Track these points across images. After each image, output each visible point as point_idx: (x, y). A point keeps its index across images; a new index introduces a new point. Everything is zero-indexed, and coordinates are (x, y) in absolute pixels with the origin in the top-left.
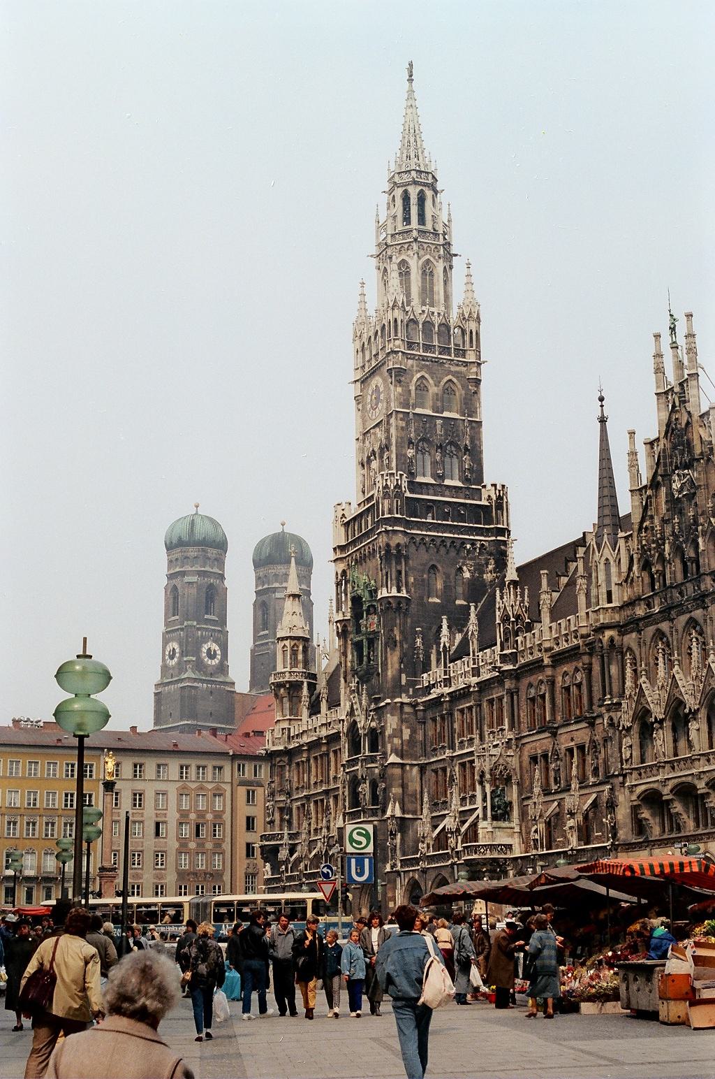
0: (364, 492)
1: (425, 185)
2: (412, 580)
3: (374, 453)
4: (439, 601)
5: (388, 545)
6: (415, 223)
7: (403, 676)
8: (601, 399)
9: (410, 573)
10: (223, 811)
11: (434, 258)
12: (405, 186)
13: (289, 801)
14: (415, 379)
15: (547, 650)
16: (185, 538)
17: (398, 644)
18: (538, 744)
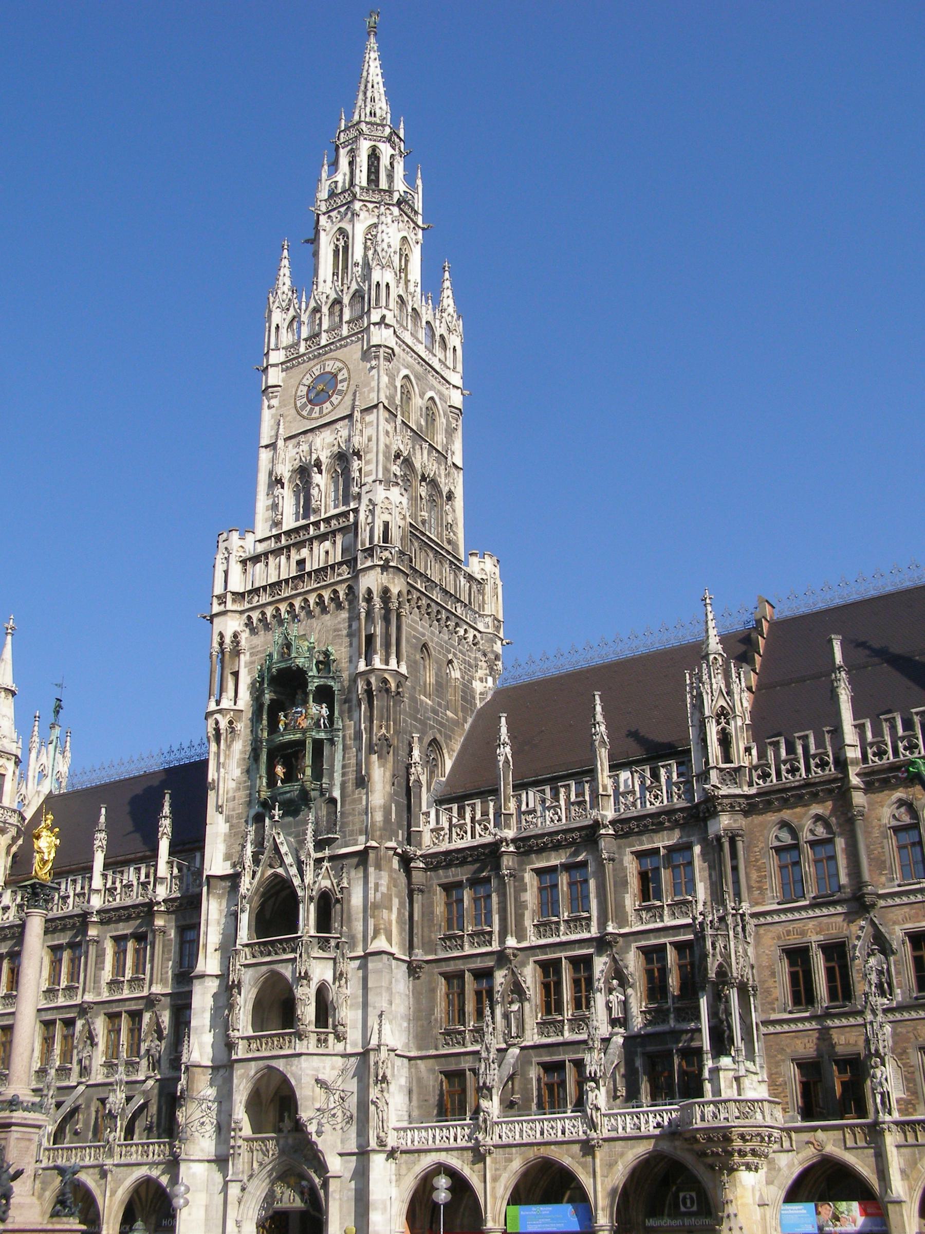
0: (277, 524)
3: (318, 464)
4: (430, 702)
5: (386, 591)
12: (375, 140)
18: (811, 924)
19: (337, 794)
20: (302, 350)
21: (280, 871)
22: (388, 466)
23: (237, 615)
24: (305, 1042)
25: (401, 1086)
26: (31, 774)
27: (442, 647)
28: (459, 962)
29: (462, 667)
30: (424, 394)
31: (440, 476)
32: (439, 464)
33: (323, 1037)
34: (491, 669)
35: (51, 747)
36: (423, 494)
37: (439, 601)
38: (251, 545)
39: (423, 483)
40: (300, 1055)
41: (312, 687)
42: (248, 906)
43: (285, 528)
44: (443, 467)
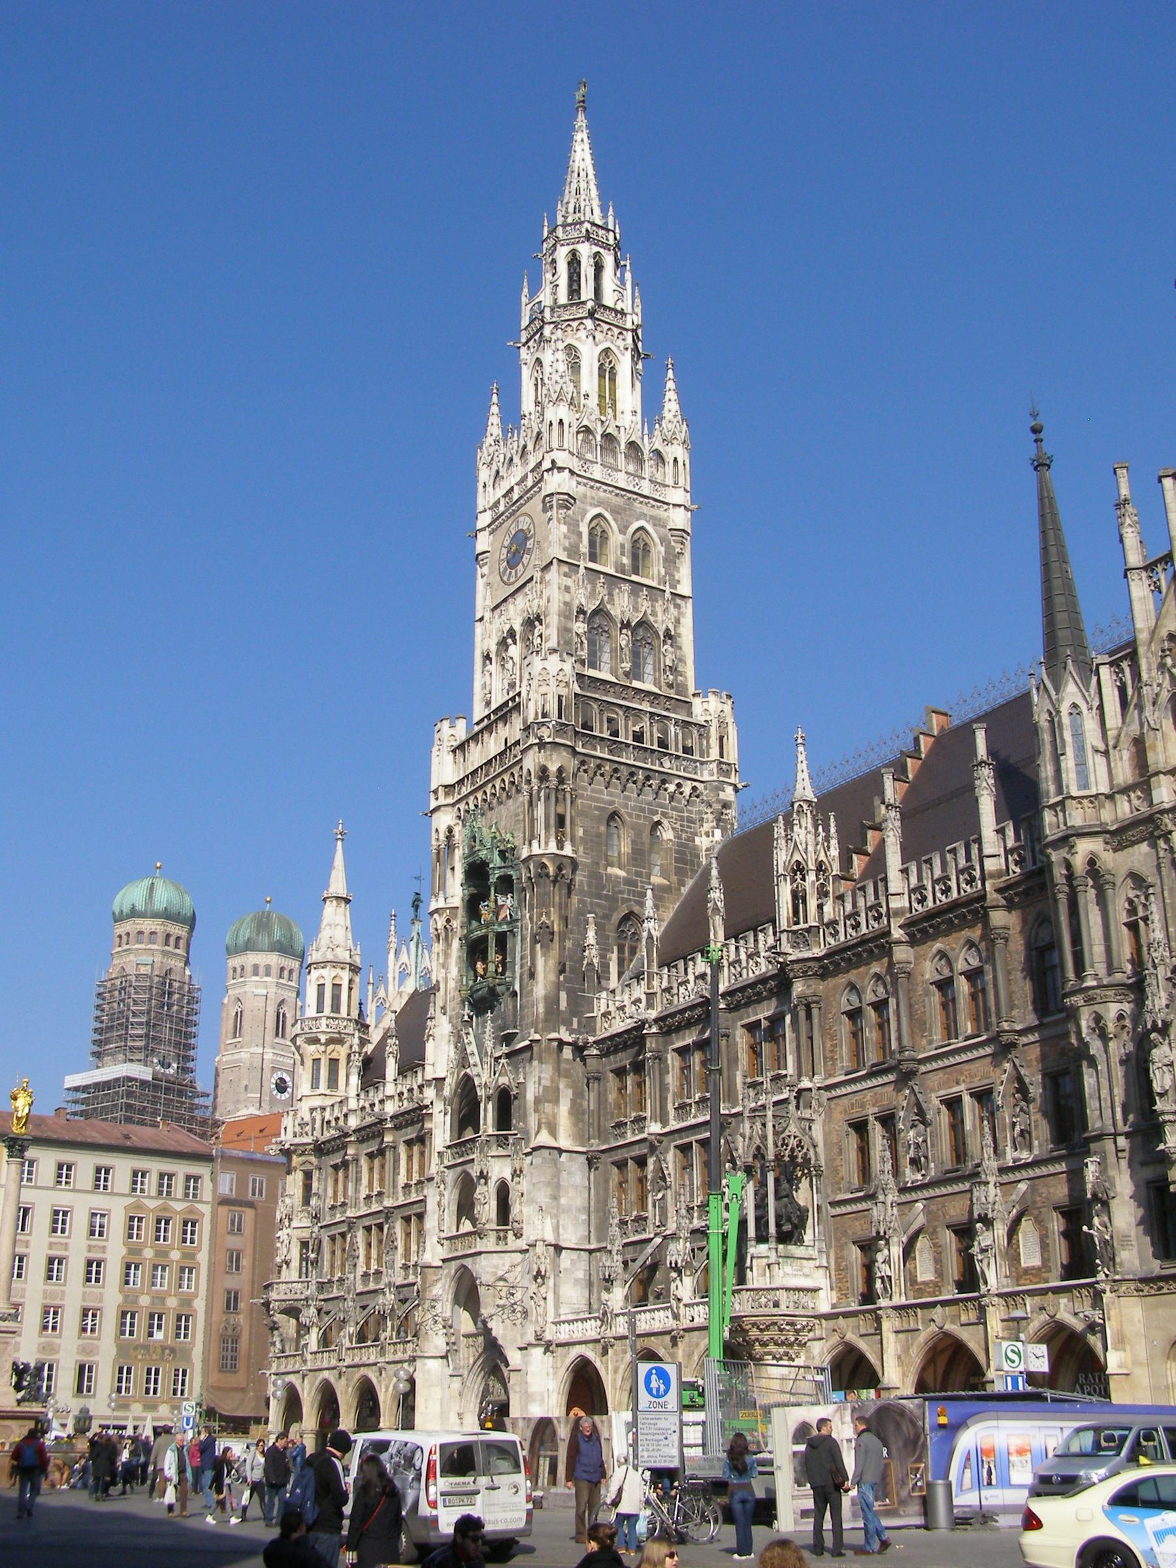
0: (488, 703)
1: (607, 247)
2: (580, 832)
3: (512, 633)
4: (622, 873)
5: (544, 770)
6: (587, 292)
7: (563, 996)
8: (1036, 430)
9: (578, 821)
10: (199, 1249)
11: (618, 347)
13: (316, 1229)
14: (589, 517)
15: (899, 913)
16: (140, 907)
17: (556, 938)
18: (869, 1094)
19: (517, 988)
20: (502, 508)
21: (468, 1071)
22: (569, 624)
23: (450, 809)
24: (484, 1240)
25: (577, 1281)
26: (390, 975)
27: (642, 810)
28: (624, 1150)
29: (677, 826)
30: (627, 527)
31: (654, 614)
32: (653, 600)
33: (502, 1234)
34: (719, 820)
35: (413, 945)
36: (623, 643)
37: (631, 762)
38: (461, 731)
39: (624, 631)
40: (480, 1253)
41: (493, 879)
42: (449, 1108)
43: (494, 706)
44: (660, 602)
